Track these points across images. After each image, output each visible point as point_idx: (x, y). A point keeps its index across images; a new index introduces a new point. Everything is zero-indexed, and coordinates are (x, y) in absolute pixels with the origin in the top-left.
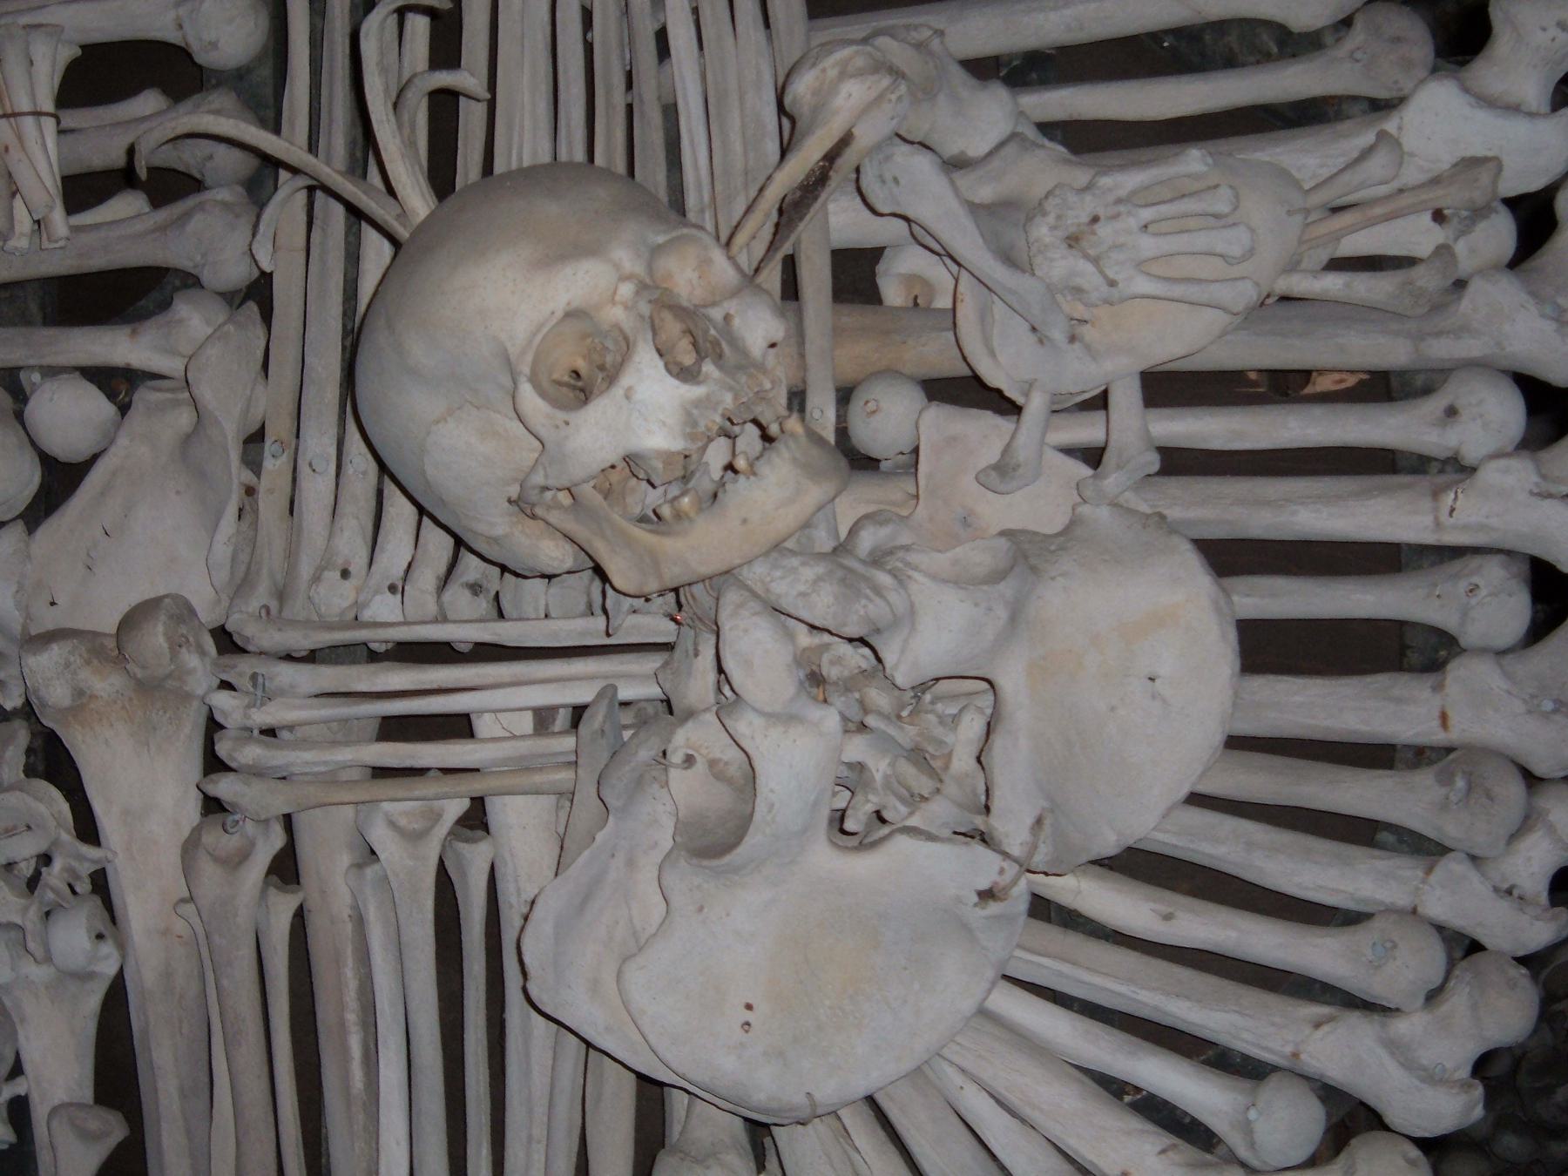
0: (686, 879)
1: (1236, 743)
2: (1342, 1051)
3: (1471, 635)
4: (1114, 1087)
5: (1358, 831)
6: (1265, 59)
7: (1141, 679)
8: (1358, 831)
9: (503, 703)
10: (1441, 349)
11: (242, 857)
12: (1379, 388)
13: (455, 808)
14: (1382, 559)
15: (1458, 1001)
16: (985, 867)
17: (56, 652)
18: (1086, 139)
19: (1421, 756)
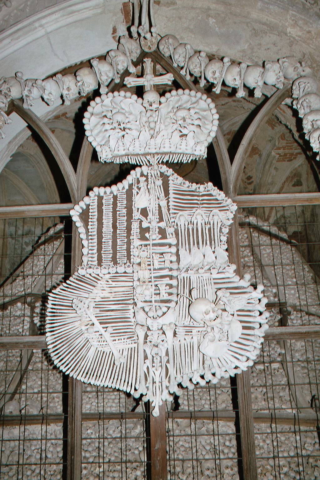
0: (209, 343)
1: (242, 334)
2: (248, 354)
3: (256, 328)
4: (233, 356)
5: (248, 340)
6: (243, 289)
7: (237, 330)
8: (248, 340)
9: (195, 331)
10: (254, 309)
11: (177, 340)
12: (249, 311)
13: (191, 337)
14: (250, 322)
15: (255, 351)
16: (228, 343)
17: (165, 326)
18: (231, 293)
19: (252, 335)
